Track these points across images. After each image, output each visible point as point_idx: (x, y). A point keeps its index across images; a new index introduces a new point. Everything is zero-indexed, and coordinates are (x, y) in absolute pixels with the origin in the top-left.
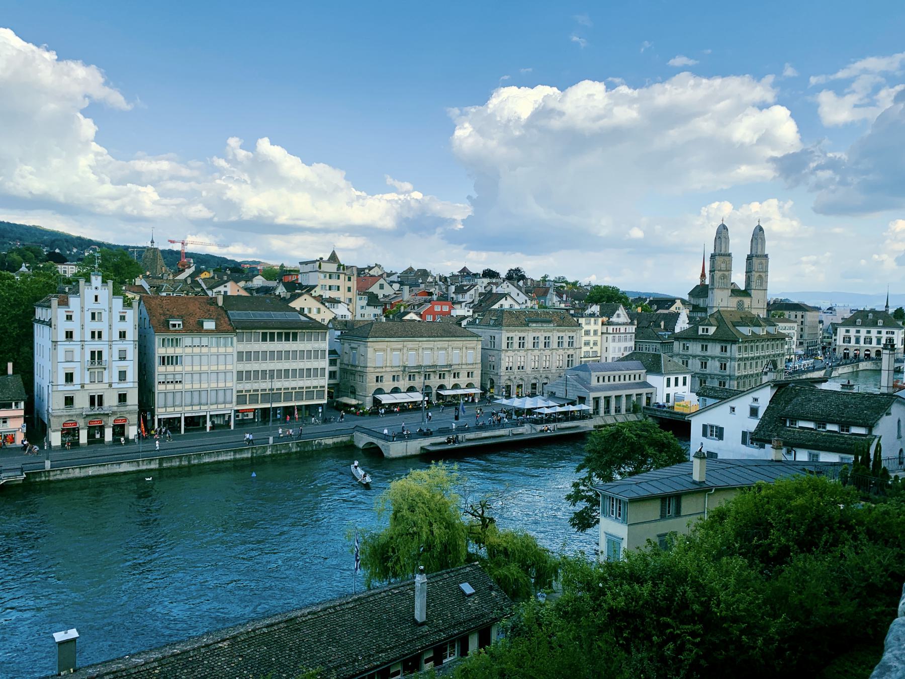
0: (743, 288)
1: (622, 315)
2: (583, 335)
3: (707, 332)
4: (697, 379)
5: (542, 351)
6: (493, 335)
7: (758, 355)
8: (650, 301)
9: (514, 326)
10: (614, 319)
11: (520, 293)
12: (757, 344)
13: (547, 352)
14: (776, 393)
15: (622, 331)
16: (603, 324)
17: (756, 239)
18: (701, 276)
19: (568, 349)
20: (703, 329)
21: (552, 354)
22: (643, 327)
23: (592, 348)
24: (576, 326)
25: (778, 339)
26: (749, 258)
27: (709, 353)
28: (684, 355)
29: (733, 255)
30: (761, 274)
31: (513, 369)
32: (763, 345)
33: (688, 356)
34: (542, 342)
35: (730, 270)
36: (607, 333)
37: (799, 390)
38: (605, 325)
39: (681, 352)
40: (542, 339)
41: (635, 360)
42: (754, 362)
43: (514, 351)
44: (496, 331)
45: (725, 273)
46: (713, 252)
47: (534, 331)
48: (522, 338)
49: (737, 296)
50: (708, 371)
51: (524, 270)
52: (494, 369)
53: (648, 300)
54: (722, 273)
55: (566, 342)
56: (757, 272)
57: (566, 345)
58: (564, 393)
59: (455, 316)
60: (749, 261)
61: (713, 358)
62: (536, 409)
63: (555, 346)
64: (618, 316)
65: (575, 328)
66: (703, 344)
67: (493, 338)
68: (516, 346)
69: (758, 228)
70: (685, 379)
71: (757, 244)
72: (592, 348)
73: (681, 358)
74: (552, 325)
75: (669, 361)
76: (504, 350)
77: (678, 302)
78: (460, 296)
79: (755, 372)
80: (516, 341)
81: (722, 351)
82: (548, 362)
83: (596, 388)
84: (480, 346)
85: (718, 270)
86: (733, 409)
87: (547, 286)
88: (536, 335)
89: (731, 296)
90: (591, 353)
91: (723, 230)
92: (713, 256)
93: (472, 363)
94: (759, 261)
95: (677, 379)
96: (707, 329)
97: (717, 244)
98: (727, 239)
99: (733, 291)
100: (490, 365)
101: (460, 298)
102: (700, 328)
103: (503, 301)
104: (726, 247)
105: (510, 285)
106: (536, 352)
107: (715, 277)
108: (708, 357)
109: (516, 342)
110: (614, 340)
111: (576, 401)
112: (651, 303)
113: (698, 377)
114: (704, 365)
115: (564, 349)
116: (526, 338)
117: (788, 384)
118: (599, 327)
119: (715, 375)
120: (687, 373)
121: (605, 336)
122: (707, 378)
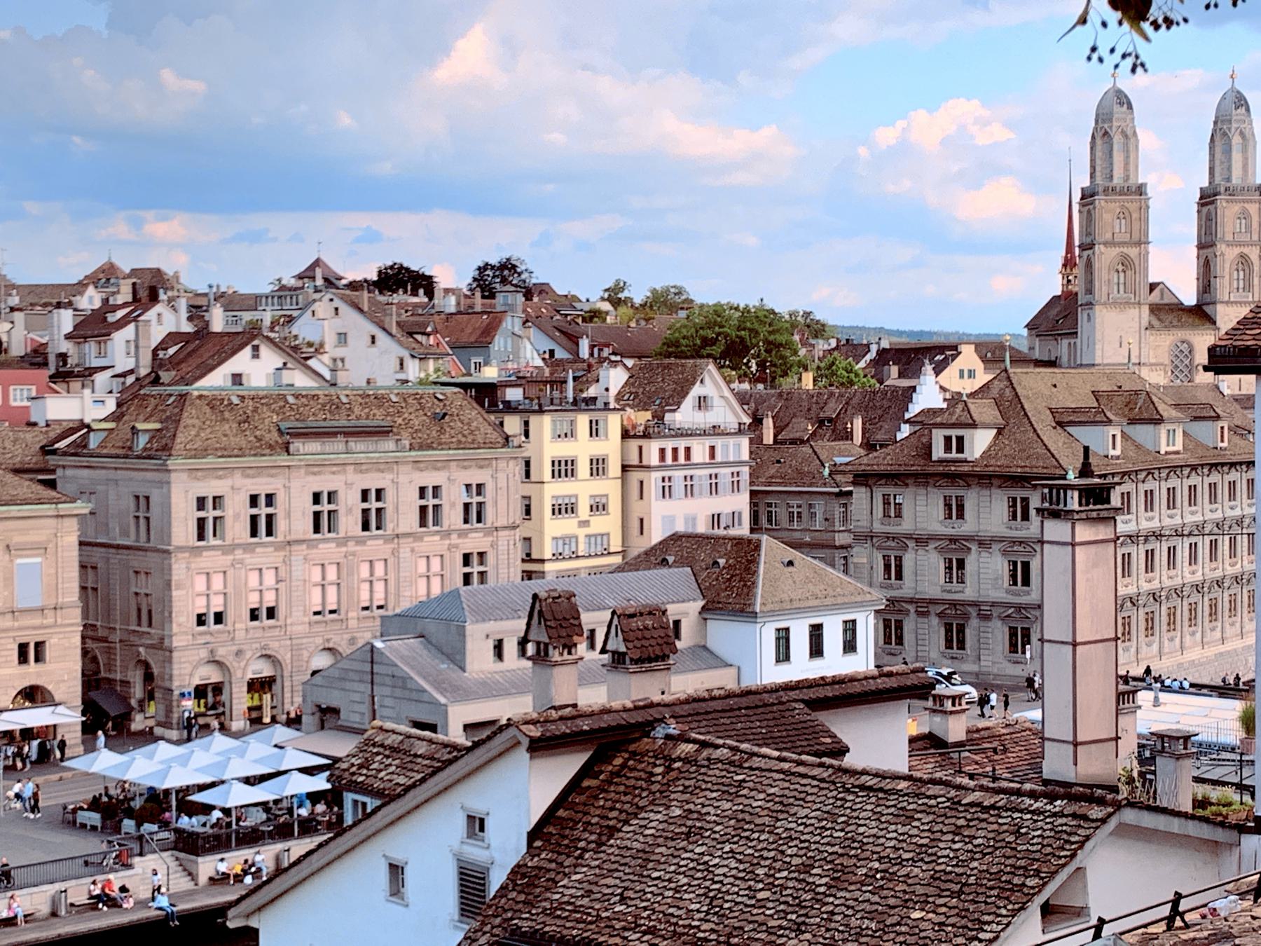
0: (1189, 297)
1: (717, 401)
2: (547, 475)
3: (960, 449)
4: (935, 621)
6: (142, 492)
7: (1198, 518)
8: (882, 353)
9: (225, 452)
10: (685, 415)
11: (381, 335)
12: (1192, 482)
13: (375, 545)
14: (574, 785)
15: (700, 454)
16: (626, 435)
17: (1225, 134)
18: (1065, 266)
19: (462, 534)
20: (948, 439)
21: (395, 552)
22: (793, 442)
23: (585, 524)
24: (491, 445)
25: (1233, 465)
26: (1207, 199)
27: (967, 527)
28: (889, 537)
30: (1246, 250)
31: (229, 618)
32: (1192, 489)
33: (902, 540)
34: (350, 511)
36: (642, 467)
37: (686, 760)
38: (635, 437)
39: (878, 527)
41: (679, 563)
43: (229, 549)
44: (149, 475)
45: (1125, 250)
46: (1087, 183)
47: (315, 467)
48: (430, 492)
49: (1169, 327)
50: (969, 592)
51: (531, 268)
52: (150, 625)
53: (874, 348)
54: (1118, 250)
55: (453, 505)
57: (452, 516)
59: (42, 424)
60: (1205, 209)
62: (202, 788)
64: (702, 403)
65: (483, 453)
66: (948, 492)
67: (142, 500)
68: (237, 528)
69: (1231, 98)
70: (850, 629)
71: (1228, 151)
72: (585, 524)
73: (879, 548)
74: (389, 444)
75: (790, 563)
76: (181, 549)
77: (968, 351)
78: (91, 347)
79: (1146, 587)
80: (236, 514)
81: (1014, 517)
82: (379, 587)
83: (484, 683)
84: (72, 540)
85: (1105, 244)
86: (396, 870)
87: (499, 309)
88: (324, 483)
89: (1150, 327)
90: (582, 540)
91: (1117, 108)
92: (1088, 196)
93: (38, 603)
94: (1236, 208)
95: (816, 632)
96: (960, 440)
97: (1099, 154)
98: (1129, 137)
99: (1155, 309)
100: (139, 610)
101: (90, 354)
102: (938, 437)
103: (241, 362)
104: (1127, 164)
105: (345, 309)
106: (327, 549)
107: (1096, 265)
108: (969, 539)
109: (237, 516)
110: (666, 492)
111: (447, 735)
112: (884, 357)
113: (940, 615)
114: (956, 568)
115: (447, 534)
116: (280, 499)
117: (645, 728)
118: (610, 446)
119: (993, 604)
120: (860, 605)
121: (635, 476)
122: (966, 617)
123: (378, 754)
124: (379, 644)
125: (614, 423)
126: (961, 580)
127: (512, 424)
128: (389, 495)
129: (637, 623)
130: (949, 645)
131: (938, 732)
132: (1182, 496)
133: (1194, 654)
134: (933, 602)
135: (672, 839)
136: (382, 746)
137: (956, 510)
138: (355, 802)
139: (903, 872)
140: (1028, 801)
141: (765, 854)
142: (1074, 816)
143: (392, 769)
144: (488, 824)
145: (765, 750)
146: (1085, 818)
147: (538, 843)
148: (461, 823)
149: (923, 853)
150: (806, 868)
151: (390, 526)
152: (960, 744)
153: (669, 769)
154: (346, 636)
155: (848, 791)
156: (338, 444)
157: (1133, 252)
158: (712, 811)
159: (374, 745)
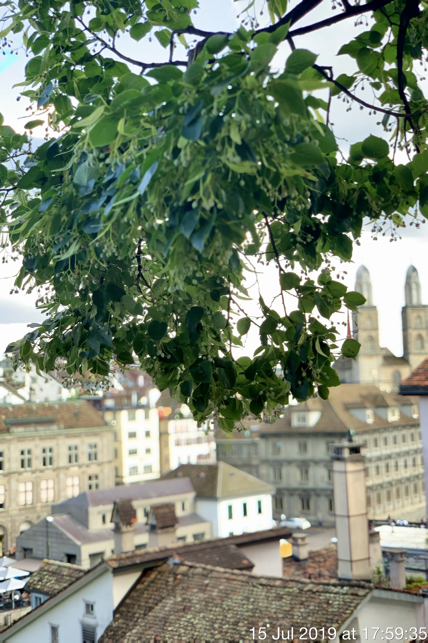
0: (399, 353)
5: (38, 474)
14: (133, 589)
19: (88, 466)
26: (404, 310)
27: (309, 455)
29: (378, 308)
35: (376, 329)
40: (37, 453)
42: (382, 464)
47: (21, 439)
50: (310, 485)
56: (416, 329)
57: (84, 459)
58: (44, 548)
61: (316, 462)
63: (63, 461)
65: (96, 430)
74: (54, 427)
86: (54, 630)
88: (25, 446)
113: (300, 495)
117: (165, 560)
123: (46, 575)
124: (50, 519)
125: (154, 413)
126: (307, 479)
127: (108, 416)
128: (55, 450)
129: (161, 511)
130: (303, 508)
131: (296, 554)
132: (399, 439)
133: (409, 509)
134: (295, 490)
135: (177, 612)
136: (48, 571)
137: (304, 448)
138: (36, 598)
139: (279, 623)
140: (332, 588)
141: (218, 617)
142: (352, 594)
143: (53, 582)
144: (95, 607)
145: (218, 569)
146: (357, 595)
147: (118, 616)
148: (82, 608)
149: (288, 614)
150: (236, 623)
151: (55, 465)
152: (305, 560)
153: (175, 579)
154: (36, 515)
155: (254, 586)
156: (32, 428)
157: (373, 334)
158: (194, 598)
159: (45, 571)
